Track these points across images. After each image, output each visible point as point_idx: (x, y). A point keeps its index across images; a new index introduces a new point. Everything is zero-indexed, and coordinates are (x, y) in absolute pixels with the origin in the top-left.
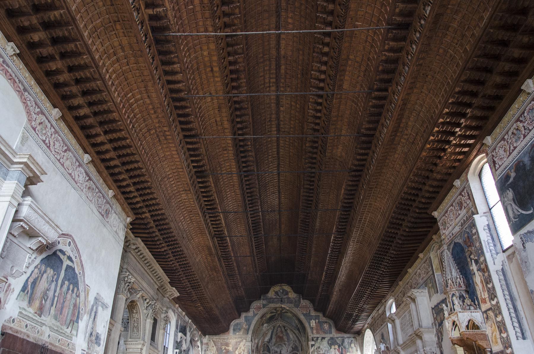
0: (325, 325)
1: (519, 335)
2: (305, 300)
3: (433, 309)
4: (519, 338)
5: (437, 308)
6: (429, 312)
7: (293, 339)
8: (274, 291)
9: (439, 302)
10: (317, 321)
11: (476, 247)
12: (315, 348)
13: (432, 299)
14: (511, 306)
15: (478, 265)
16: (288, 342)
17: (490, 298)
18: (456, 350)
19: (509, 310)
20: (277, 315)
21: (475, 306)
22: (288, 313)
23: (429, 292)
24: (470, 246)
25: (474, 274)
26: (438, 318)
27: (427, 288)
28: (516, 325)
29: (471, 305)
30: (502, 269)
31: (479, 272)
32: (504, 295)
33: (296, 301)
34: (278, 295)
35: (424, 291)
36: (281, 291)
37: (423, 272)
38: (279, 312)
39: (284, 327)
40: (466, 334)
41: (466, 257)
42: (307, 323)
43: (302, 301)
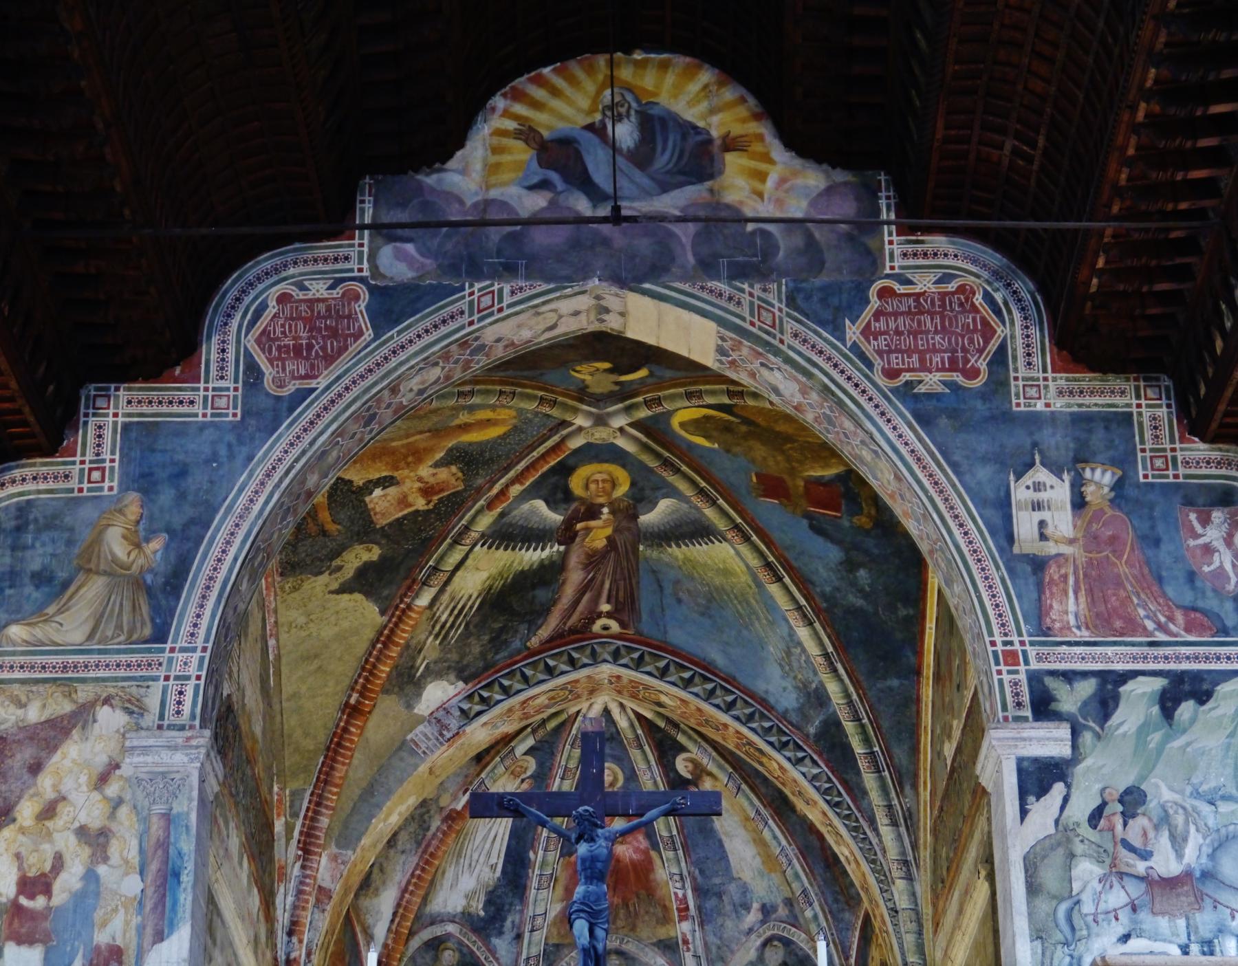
0: (1213, 534)
2: (938, 242)
7: (763, 888)
8: (527, 134)
10: (1101, 479)
12: (1080, 808)
16: (704, 919)
20: (575, 577)
22: (700, 532)
33: (812, 254)
34: (585, 184)
36: (625, 133)
38: (599, 533)
39: (666, 748)
42: (964, 507)
43: (893, 244)
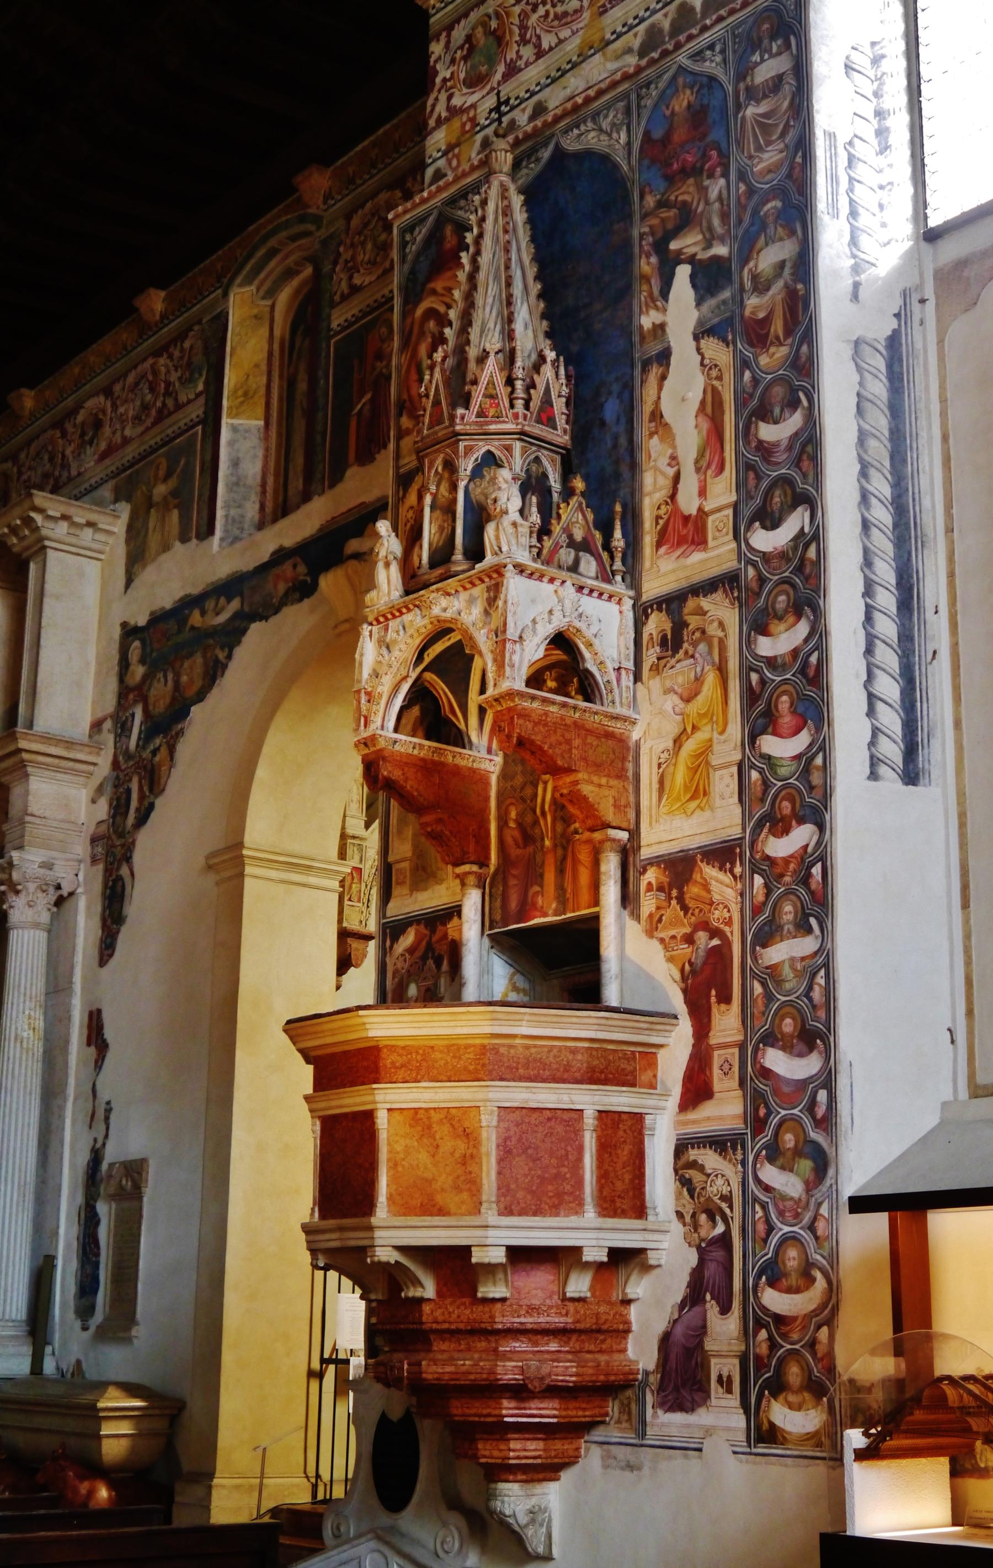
1: (892, 750)
3: (129, 632)
4: (883, 770)
5: (172, 625)
6: (92, 653)
9: (195, 591)
11: (742, 177)
13: (148, 575)
14: (885, 572)
15: (726, 294)
17: (747, 512)
18: (241, 875)
19: (868, 591)
21: (605, 555)
23: (135, 534)
24: (695, 171)
25: (664, 357)
26: (161, 691)
27: (124, 510)
28: (889, 688)
29: (584, 546)
30: (894, 341)
31: (712, 347)
32: (865, 497)
35: (103, 521)
37: (130, 410)
40: (524, 715)
41: (627, 243)
